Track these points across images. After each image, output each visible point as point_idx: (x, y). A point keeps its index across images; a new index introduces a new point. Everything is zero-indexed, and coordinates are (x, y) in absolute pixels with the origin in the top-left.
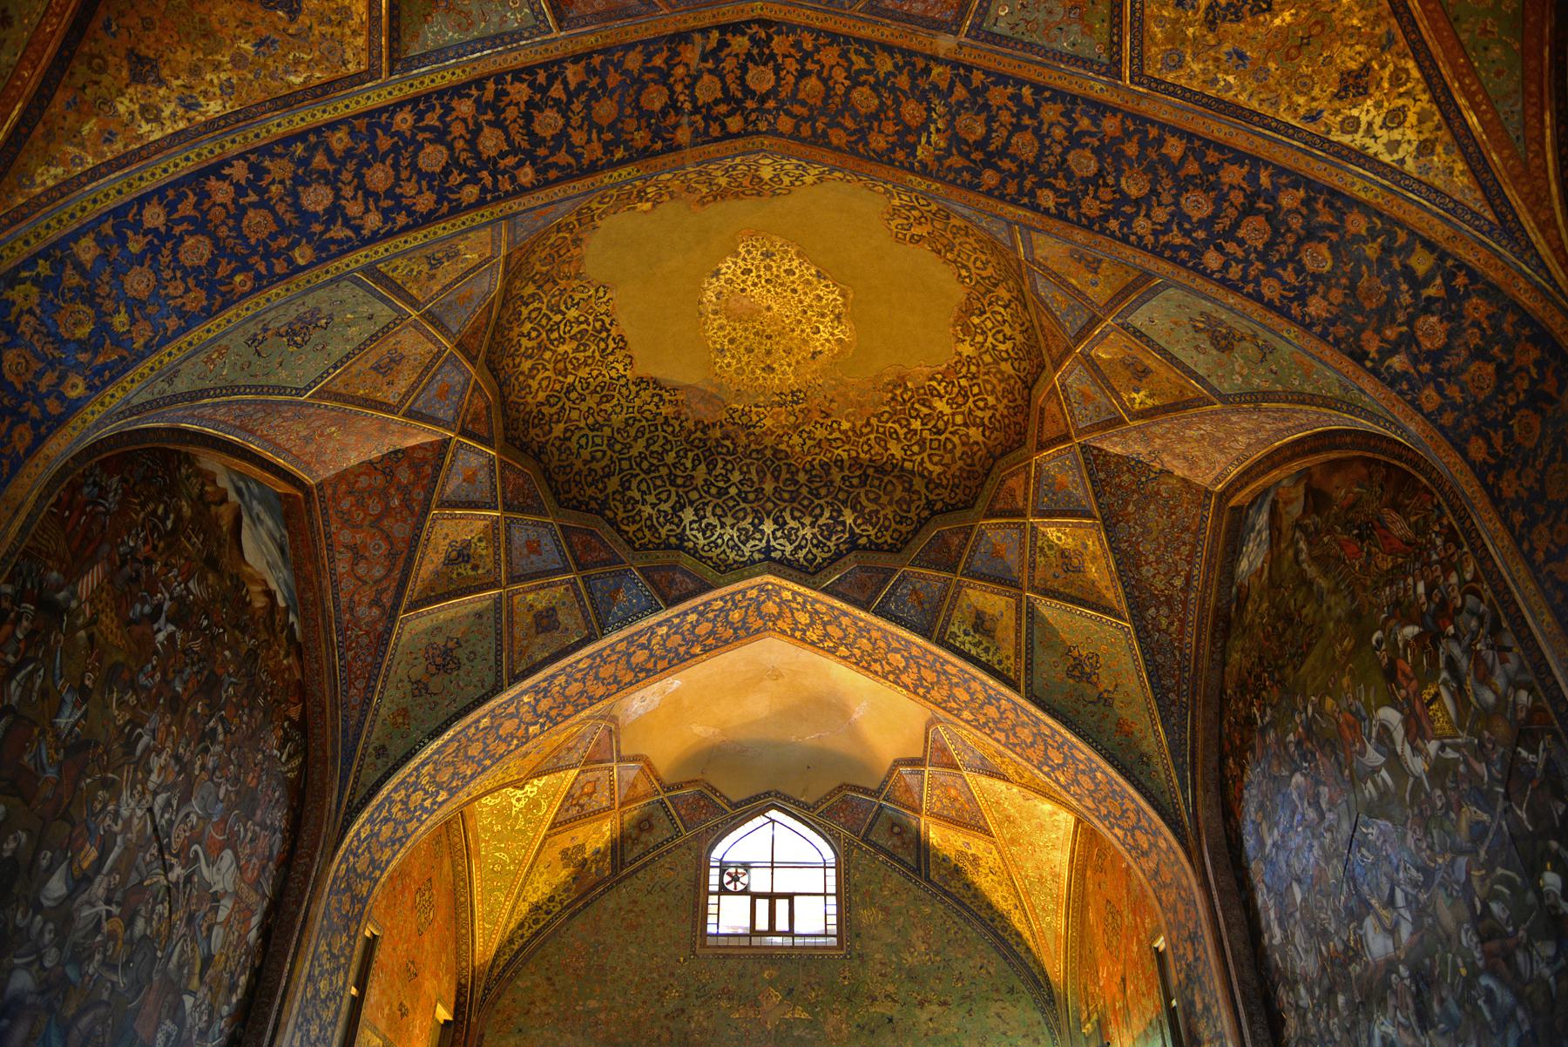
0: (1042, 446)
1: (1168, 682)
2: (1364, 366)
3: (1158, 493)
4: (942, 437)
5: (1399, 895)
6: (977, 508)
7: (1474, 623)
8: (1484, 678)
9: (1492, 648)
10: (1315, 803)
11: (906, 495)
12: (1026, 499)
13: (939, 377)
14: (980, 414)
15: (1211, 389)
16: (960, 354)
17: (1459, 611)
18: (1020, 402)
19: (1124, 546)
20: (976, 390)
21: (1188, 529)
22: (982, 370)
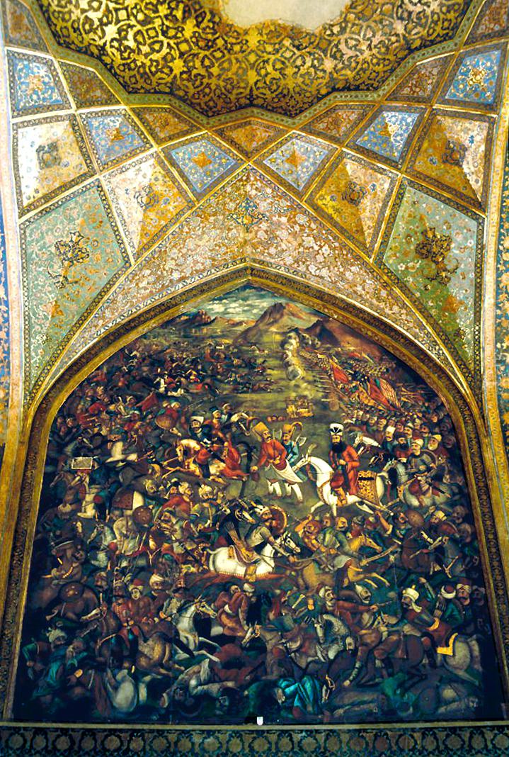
0: (221, 133)
1: (108, 314)
2: (496, 344)
3: (229, 230)
4: (161, 38)
5: (268, 550)
6: (132, 97)
7: (422, 468)
8: (416, 491)
9: (430, 485)
10: (204, 467)
11: (97, 23)
12: (171, 138)
13: (217, 19)
14: (198, 64)
15: (381, 253)
16: (246, 33)
17: (413, 456)
18: (233, 97)
19: (186, 229)
20: (218, 54)
21: (214, 260)
22: (240, 56)
